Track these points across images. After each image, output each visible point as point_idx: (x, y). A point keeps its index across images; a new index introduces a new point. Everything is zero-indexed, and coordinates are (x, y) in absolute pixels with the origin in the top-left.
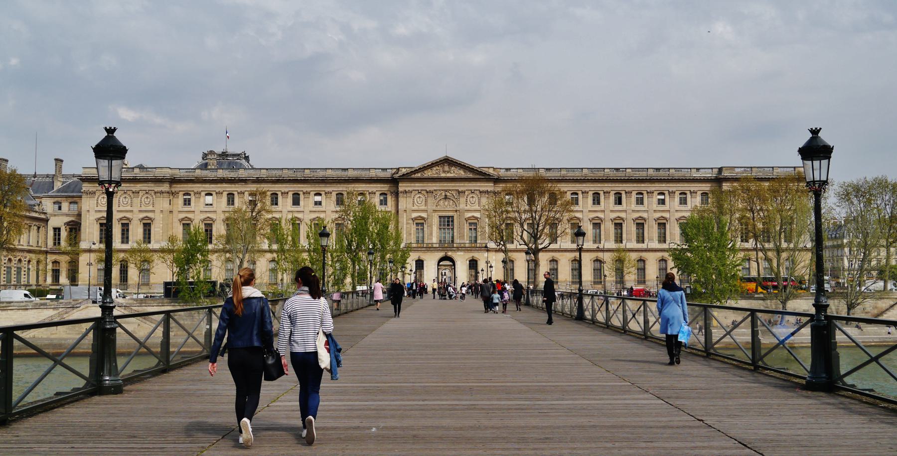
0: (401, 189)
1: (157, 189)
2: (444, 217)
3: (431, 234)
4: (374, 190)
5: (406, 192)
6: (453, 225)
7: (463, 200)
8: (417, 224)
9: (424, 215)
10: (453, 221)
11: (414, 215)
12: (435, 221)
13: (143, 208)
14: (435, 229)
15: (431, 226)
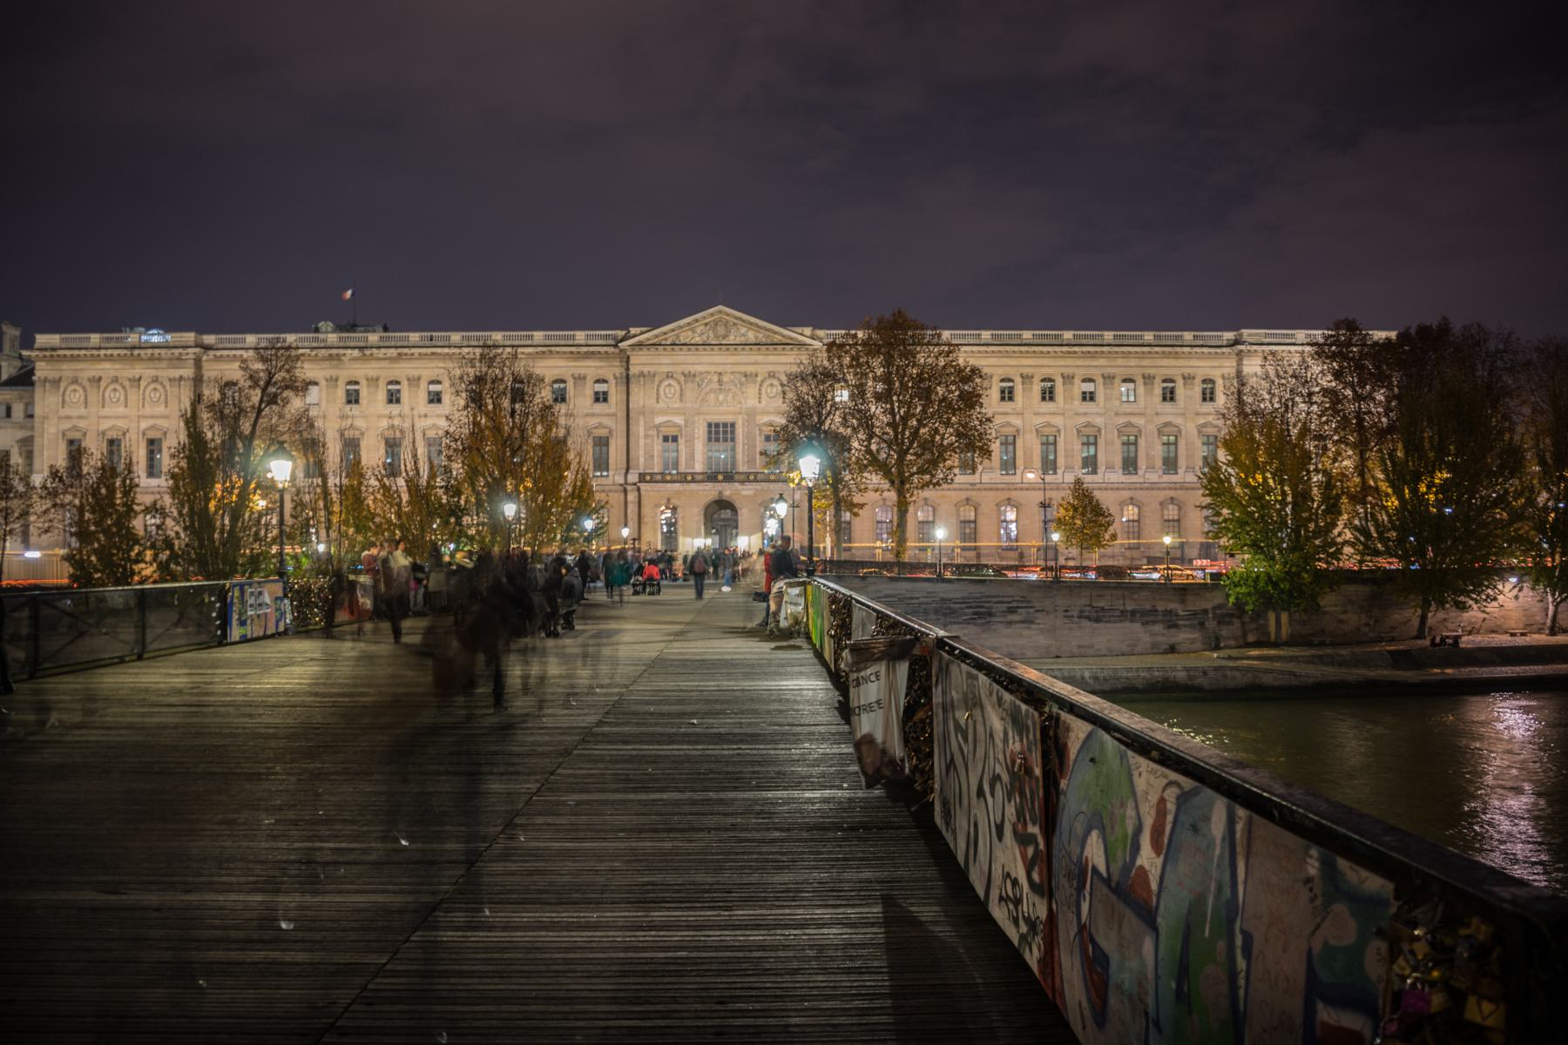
0: (634, 370)
1: (176, 373)
2: (717, 425)
3: (692, 456)
4: (582, 371)
5: (642, 374)
6: (733, 439)
7: (752, 390)
8: (666, 439)
9: (679, 420)
10: (733, 432)
11: (659, 420)
12: (701, 432)
13: (148, 410)
14: (700, 446)
15: (690, 441)
